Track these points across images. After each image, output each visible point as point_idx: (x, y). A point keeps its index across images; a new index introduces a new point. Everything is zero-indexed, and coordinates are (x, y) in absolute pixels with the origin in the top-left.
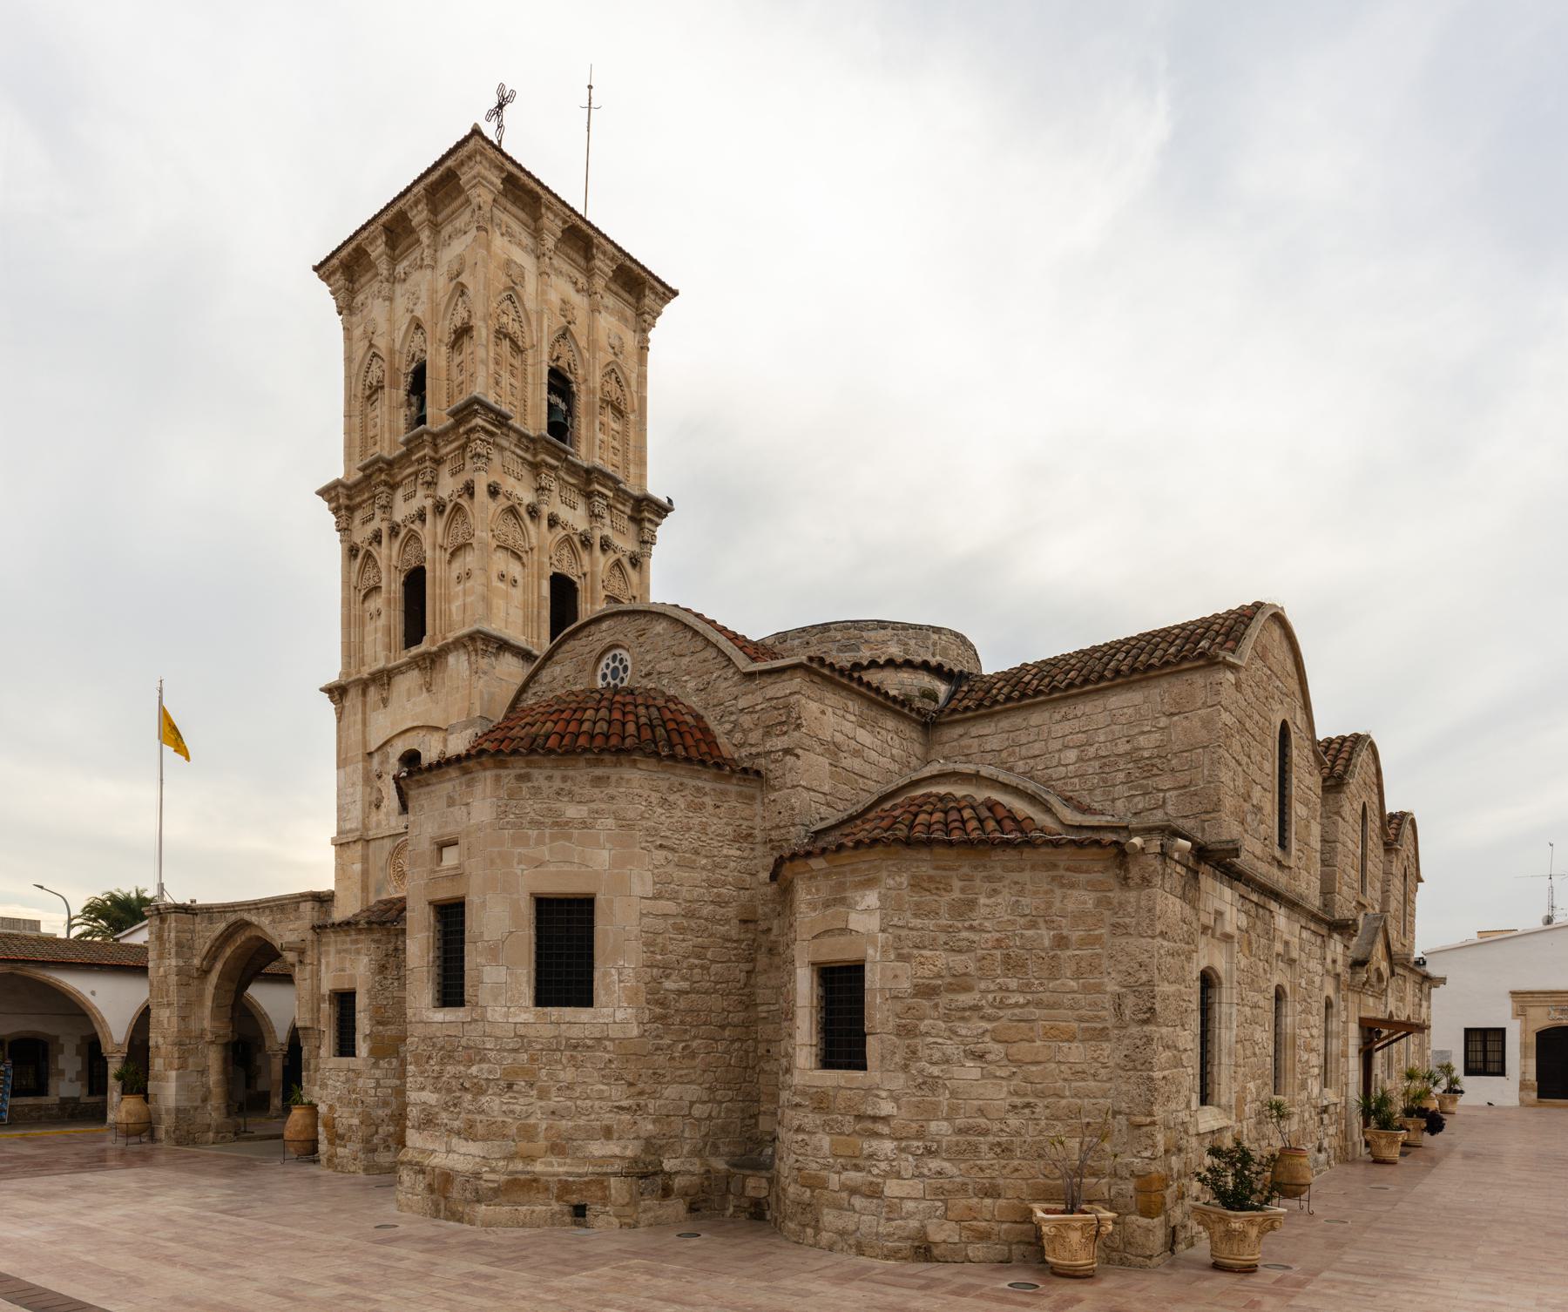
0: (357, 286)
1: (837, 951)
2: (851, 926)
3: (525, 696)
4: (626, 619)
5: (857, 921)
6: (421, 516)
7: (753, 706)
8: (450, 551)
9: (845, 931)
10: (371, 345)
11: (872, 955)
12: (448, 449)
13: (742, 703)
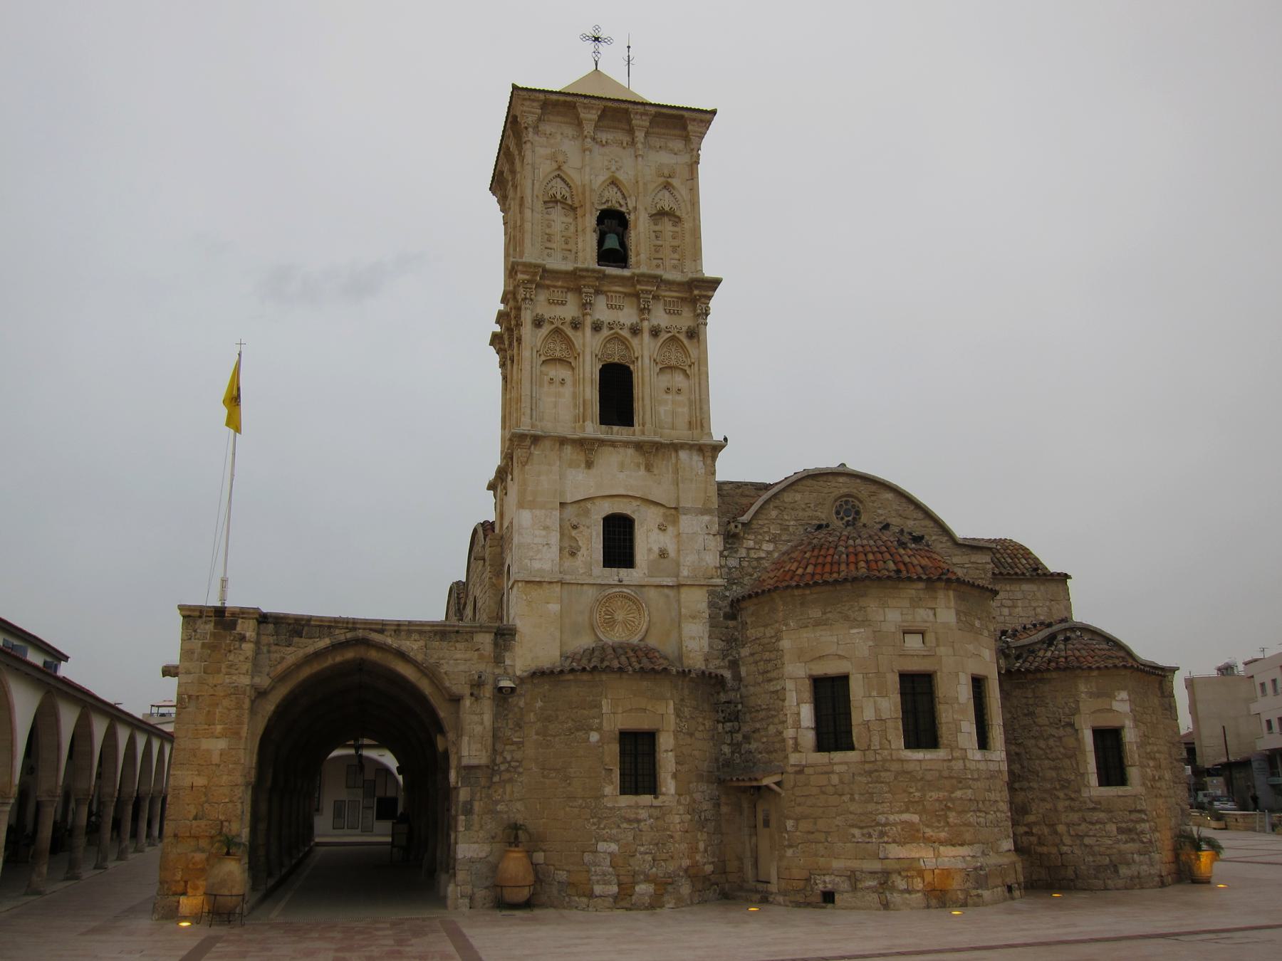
1: (1107, 721)
2: (1114, 709)
3: (767, 506)
4: (858, 481)
5: (1116, 706)
6: (635, 331)
9: (1111, 710)
10: (559, 168)
11: (1128, 723)
12: (667, 294)
13: (955, 560)
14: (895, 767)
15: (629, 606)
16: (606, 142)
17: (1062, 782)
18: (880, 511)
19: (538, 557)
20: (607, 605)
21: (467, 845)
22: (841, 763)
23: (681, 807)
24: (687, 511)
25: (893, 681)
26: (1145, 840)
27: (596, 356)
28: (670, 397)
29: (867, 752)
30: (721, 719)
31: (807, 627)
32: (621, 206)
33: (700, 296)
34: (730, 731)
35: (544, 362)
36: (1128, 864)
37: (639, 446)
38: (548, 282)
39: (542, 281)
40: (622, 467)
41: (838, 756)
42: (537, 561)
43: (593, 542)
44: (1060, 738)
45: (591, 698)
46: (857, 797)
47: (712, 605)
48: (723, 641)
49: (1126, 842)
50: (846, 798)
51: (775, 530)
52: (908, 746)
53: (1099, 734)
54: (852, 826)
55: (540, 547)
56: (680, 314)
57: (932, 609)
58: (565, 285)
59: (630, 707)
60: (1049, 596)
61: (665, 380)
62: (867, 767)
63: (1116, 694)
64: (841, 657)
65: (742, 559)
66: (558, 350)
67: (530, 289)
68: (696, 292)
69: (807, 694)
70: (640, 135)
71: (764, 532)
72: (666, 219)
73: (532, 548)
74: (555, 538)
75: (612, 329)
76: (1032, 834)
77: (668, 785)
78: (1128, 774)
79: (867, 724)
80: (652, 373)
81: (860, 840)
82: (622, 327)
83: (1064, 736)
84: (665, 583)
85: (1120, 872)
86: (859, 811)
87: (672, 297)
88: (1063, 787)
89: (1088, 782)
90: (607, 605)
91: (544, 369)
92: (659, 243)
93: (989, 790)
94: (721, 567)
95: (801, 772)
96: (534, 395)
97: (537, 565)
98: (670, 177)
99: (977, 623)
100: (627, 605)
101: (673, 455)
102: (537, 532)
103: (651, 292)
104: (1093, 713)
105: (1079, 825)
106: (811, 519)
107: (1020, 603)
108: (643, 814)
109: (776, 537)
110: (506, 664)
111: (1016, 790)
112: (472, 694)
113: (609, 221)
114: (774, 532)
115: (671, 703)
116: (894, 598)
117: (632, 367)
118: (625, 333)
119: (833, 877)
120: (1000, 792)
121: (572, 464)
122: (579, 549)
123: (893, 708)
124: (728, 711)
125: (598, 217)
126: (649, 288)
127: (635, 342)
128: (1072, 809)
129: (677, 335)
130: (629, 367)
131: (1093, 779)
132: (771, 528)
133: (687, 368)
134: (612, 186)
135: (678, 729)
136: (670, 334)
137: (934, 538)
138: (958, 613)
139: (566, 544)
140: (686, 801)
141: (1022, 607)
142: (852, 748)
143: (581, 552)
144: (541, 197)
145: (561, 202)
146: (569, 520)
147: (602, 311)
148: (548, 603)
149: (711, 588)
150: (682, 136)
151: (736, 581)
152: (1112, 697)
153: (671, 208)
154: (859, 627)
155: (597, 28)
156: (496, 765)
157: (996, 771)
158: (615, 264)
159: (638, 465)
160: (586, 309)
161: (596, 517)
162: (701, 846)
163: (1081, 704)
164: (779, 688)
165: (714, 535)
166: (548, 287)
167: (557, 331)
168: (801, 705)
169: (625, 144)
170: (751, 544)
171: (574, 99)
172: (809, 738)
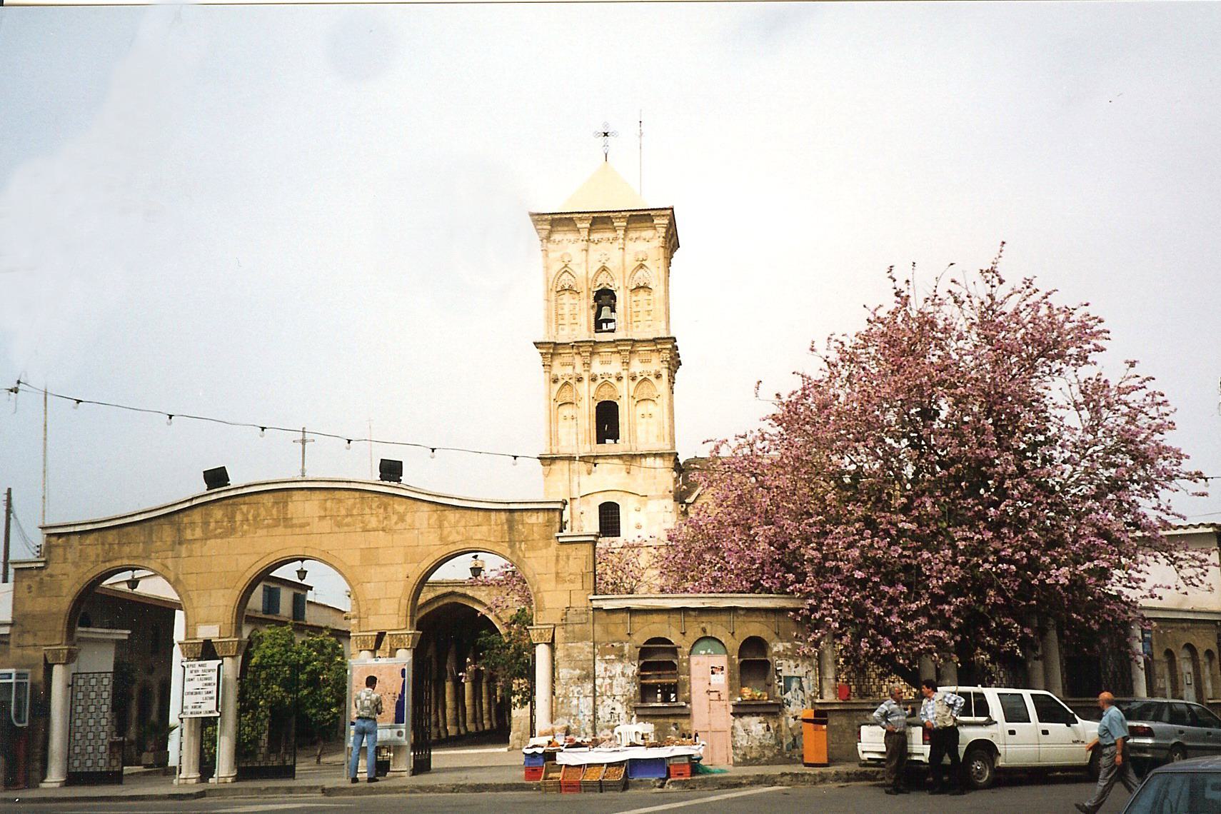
0: (555, 229)
24: (652, 498)
37: (619, 457)
61: (643, 408)
68: (659, 346)
72: (641, 290)
98: (643, 260)
118: (613, 380)
127: (618, 385)
133: (655, 399)
144: (554, 289)
147: (597, 367)
155: (606, 125)
159: (621, 469)
167: (566, 383)
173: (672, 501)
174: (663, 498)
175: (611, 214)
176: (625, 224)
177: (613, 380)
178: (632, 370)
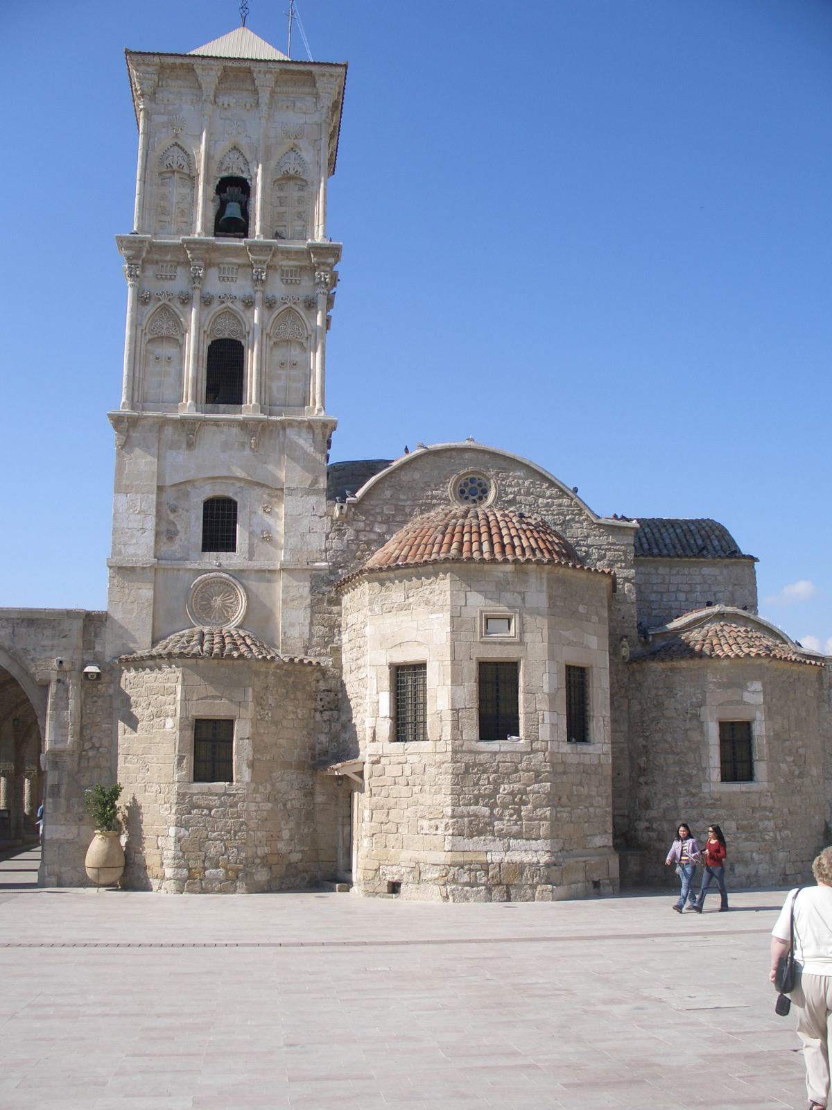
2: (745, 699)
3: (382, 486)
4: (487, 457)
5: (748, 697)
7: (600, 545)
8: (274, 340)
9: (741, 702)
12: (285, 263)
14: (468, 758)
15: (227, 592)
16: (228, 105)
17: (685, 777)
18: (510, 490)
19: (134, 541)
20: (204, 590)
21: (54, 826)
22: (412, 754)
23: (258, 795)
25: (471, 670)
26: (767, 838)
27: (205, 332)
28: (284, 372)
29: (438, 743)
30: (319, 707)
31: (391, 612)
32: (242, 172)
33: (319, 264)
34: (328, 720)
35: (150, 341)
36: (746, 863)
38: (156, 257)
39: (150, 256)
40: (226, 446)
41: (412, 746)
42: (132, 546)
43: (193, 526)
44: (686, 730)
45: (169, 684)
46: (427, 788)
47: (313, 589)
48: (325, 627)
49: (746, 840)
50: (417, 789)
51: (388, 511)
52: (485, 735)
53: (725, 727)
54: (423, 817)
55: (135, 532)
56: (299, 284)
57: (520, 593)
58: (175, 259)
59: (205, 695)
60: (732, 580)
61: (279, 355)
62: (438, 758)
63: (748, 684)
64: (420, 644)
65: (350, 542)
66: (165, 326)
67: (135, 265)
69: (386, 683)
70: (265, 96)
71: (378, 513)
72: (291, 183)
73: (126, 533)
74: (151, 523)
75: (224, 302)
76: (653, 830)
77: (242, 771)
78: (755, 768)
79: (439, 713)
80: (264, 348)
81: (427, 832)
82: (233, 299)
83: (690, 729)
84: (266, 567)
85: (737, 871)
86: (429, 802)
87: (290, 266)
88: (686, 783)
89: (710, 778)
90: (204, 590)
91: (150, 347)
92: (282, 209)
93: (581, 784)
94: (326, 551)
95: (378, 762)
96: (137, 375)
97: (131, 550)
99: (581, 609)
100: (226, 590)
101: (281, 432)
102: (132, 517)
103: (264, 262)
104: (719, 705)
105: (697, 821)
106: (432, 499)
107: (699, 588)
108: (215, 801)
109: (389, 518)
110: (96, 649)
111: (641, 784)
112: (59, 681)
113: (231, 189)
114: (387, 513)
115: (250, 690)
116: (478, 581)
117: (243, 342)
118: (238, 307)
119: (400, 868)
120: (597, 787)
121: (173, 446)
122: (176, 533)
123: (468, 698)
124: (328, 699)
125: (217, 186)
126: (262, 258)
128: (692, 806)
129: (293, 306)
130: (241, 342)
131: (715, 774)
132: (385, 508)
133: (303, 341)
134: (234, 151)
135: (259, 717)
136: (286, 306)
137: (567, 518)
138: (551, 598)
139: (163, 527)
140: (266, 789)
141: (700, 593)
142: (425, 739)
143: (179, 536)
145: (178, 172)
146: (168, 504)
148: (139, 589)
149: (314, 572)
150: (312, 94)
151: (342, 565)
152: (743, 687)
153: (297, 171)
154: (438, 611)
156: (84, 751)
157: (594, 765)
158: (232, 234)
160: (194, 283)
161: (195, 500)
162: (286, 834)
163: (708, 695)
164: (364, 675)
165: (321, 517)
166: (157, 263)
167: (165, 308)
168: (381, 693)
169: (248, 106)
170: (361, 525)
171: (193, 61)
172: (385, 727)
173: (324, 499)
174: (308, 494)
175: (252, 64)
176: (273, 84)
177: (238, 307)
178: (269, 293)
